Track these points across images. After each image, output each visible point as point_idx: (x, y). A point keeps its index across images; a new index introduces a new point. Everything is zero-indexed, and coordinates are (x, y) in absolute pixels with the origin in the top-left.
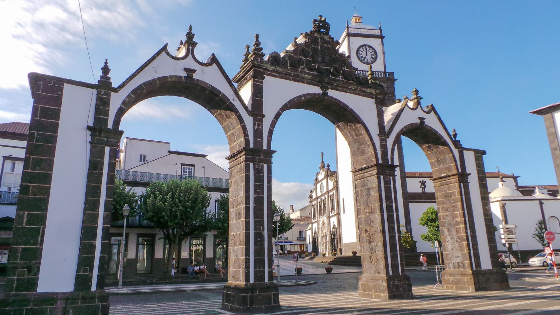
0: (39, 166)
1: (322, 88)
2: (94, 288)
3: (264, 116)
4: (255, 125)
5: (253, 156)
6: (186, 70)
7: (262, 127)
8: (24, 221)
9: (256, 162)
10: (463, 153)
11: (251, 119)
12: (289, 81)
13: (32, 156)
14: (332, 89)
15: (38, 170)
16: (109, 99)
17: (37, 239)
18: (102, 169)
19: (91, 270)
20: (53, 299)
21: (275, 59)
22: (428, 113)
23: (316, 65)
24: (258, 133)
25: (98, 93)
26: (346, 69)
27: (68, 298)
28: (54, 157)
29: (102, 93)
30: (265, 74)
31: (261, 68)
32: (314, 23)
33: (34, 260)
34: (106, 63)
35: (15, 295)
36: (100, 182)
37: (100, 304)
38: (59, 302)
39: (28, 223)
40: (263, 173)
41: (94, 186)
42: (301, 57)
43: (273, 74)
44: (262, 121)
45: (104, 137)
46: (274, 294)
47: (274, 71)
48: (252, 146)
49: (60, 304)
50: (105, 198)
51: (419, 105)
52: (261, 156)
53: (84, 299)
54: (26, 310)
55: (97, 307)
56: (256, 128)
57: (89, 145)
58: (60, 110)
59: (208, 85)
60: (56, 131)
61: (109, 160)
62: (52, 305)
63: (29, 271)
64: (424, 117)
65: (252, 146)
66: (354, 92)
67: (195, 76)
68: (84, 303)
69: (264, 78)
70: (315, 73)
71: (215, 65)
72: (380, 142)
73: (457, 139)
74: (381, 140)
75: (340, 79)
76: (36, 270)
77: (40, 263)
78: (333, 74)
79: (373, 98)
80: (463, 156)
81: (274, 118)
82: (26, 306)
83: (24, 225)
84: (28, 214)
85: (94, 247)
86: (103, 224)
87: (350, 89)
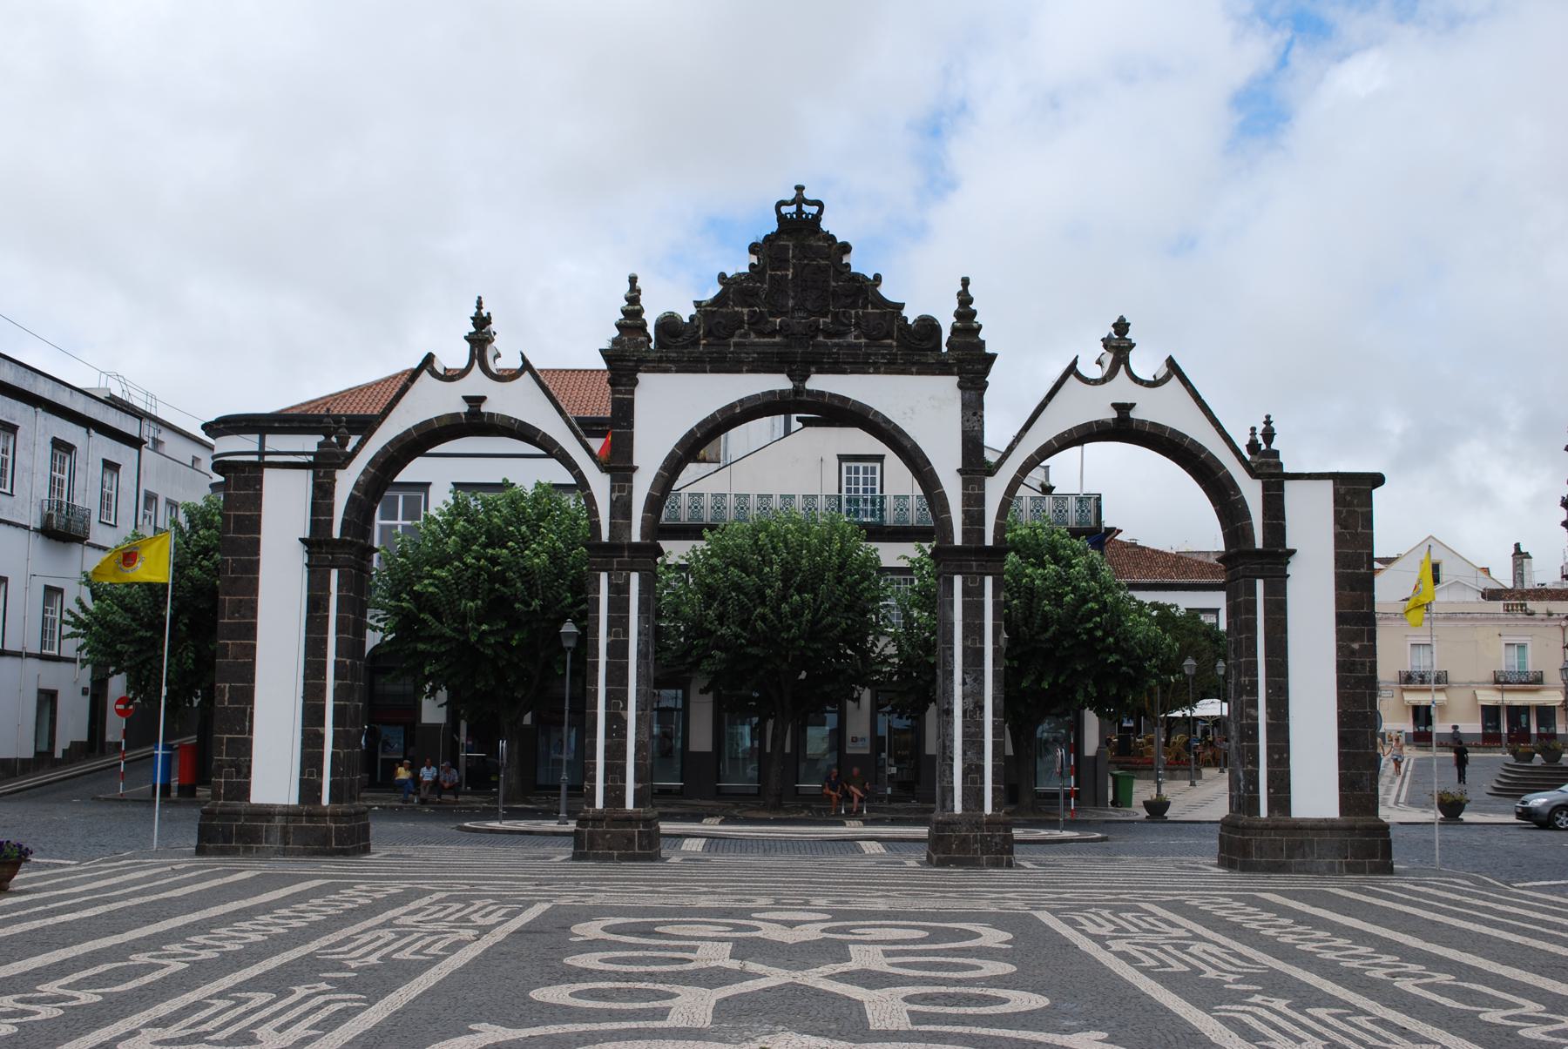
0: (238, 612)
2: (325, 800)
3: (634, 469)
4: (612, 490)
6: (467, 399)
7: (630, 493)
9: (612, 570)
11: (606, 478)
17: (245, 725)
18: (327, 609)
19: (321, 774)
20: (269, 814)
21: (668, 324)
22: (1155, 384)
23: (778, 320)
24: (621, 508)
26: (870, 310)
27: (288, 813)
28: (257, 595)
29: (321, 474)
30: (640, 371)
31: (630, 361)
35: (223, 805)
36: (326, 632)
37: (333, 825)
38: (277, 817)
39: (231, 701)
40: (627, 592)
41: (315, 639)
42: (736, 309)
43: (659, 365)
44: (630, 480)
45: (327, 553)
47: (660, 360)
48: (605, 537)
49: (278, 822)
50: (334, 657)
51: (1122, 366)
52: (623, 557)
55: (329, 829)
56: (615, 496)
57: (306, 569)
58: (260, 516)
59: (513, 421)
60: (257, 553)
62: (268, 822)
63: (239, 773)
65: (605, 537)
66: (894, 366)
67: (485, 408)
69: (636, 382)
70: (777, 339)
72: (963, 489)
73: (1274, 446)
77: (250, 761)
78: (829, 335)
79: (952, 374)
81: (661, 468)
82: (236, 821)
87: (875, 363)
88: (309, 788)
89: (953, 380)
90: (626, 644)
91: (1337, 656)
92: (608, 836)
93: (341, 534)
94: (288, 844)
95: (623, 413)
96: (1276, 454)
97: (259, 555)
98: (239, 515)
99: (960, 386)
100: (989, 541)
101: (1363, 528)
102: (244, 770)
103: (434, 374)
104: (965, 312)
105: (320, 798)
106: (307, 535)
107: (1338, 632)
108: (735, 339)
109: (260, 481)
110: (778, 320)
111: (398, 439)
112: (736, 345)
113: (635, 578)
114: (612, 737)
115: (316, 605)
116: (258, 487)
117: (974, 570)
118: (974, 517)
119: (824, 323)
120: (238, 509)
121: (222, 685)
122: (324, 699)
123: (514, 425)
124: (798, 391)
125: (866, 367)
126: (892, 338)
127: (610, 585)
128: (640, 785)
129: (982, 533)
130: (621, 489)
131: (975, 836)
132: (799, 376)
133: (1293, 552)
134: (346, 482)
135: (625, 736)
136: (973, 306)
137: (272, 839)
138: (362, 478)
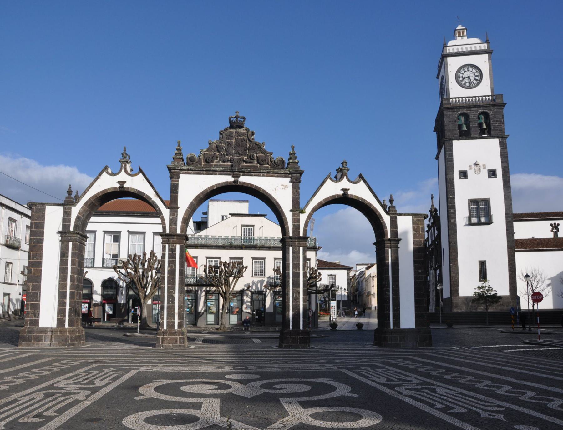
0: (36, 257)
1: (233, 177)
2: (67, 326)
4: (170, 215)
5: (168, 239)
7: (177, 216)
8: (31, 289)
10: (396, 218)
12: (202, 175)
13: (32, 252)
14: (243, 175)
15: (35, 260)
16: (70, 212)
18: (68, 257)
19: (65, 316)
23: (229, 157)
24: (173, 222)
25: (64, 209)
27: (52, 330)
28: (42, 251)
30: (181, 173)
32: (230, 120)
33: (36, 310)
34: (70, 187)
36: (67, 265)
37: (69, 335)
38: (49, 333)
40: (175, 251)
44: (177, 212)
45: (68, 236)
46: (180, 337)
48: (168, 232)
49: (49, 334)
51: (345, 177)
52: (174, 239)
53: (61, 332)
54: (34, 335)
56: (171, 218)
58: (44, 223)
59: (136, 190)
61: (72, 250)
62: (46, 334)
63: (35, 316)
64: (348, 188)
65: (168, 232)
66: (269, 174)
67: (126, 185)
68: (61, 334)
69: (179, 178)
71: (141, 174)
74: (293, 215)
75: (255, 165)
76: (38, 315)
77: (39, 312)
78: (246, 162)
79: (289, 177)
80: (396, 222)
81: (188, 208)
83: (31, 291)
84: (32, 285)
85: (65, 303)
86: (70, 290)
88: (61, 322)
89: (289, 179)
90: (175, 270)
91: (414, 274)
92: (169, 339)
93: (74, 229)
94: (52, 342)
95: (174, 189)
96: (394, 207)
97: (43, 237)
98: (36, 223)
99: (291, 181)
100: (301, 235)
101: (422, 232)
102: (37, 315)
103: (108, 173)
104: (292, 155)
105: (65, 325)
106: (60, 229)
107: (414, 266)
108: (213, 164)
109: (44, 210)
110: (229, 157)
111: (95, 196)
112: (215, 165)
113: (178, 246)
114: (170, 304)
115: (64, 255)
116: (44, 212)
117: (297, 245)
118: (296, 227)
119: (245, 158)
120: (36, 220)
121: (29, 284)
122: (66, 289)
123: (136, 192)
124: (235, 182)
125: (259, 174)
126: (268, 164)
127: (169, 249)
128: (180, 321)
129: (299, 232)
130: (174, 215)
131: (297, 337)
132: (236, 176)
133: (400, 240)
134: (75, 211)
135: (174, 303)
136: (296, 155)
137: (46, 340)
138: (81, 210)
